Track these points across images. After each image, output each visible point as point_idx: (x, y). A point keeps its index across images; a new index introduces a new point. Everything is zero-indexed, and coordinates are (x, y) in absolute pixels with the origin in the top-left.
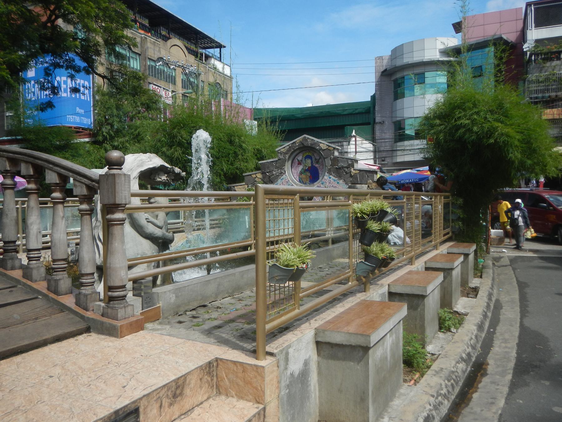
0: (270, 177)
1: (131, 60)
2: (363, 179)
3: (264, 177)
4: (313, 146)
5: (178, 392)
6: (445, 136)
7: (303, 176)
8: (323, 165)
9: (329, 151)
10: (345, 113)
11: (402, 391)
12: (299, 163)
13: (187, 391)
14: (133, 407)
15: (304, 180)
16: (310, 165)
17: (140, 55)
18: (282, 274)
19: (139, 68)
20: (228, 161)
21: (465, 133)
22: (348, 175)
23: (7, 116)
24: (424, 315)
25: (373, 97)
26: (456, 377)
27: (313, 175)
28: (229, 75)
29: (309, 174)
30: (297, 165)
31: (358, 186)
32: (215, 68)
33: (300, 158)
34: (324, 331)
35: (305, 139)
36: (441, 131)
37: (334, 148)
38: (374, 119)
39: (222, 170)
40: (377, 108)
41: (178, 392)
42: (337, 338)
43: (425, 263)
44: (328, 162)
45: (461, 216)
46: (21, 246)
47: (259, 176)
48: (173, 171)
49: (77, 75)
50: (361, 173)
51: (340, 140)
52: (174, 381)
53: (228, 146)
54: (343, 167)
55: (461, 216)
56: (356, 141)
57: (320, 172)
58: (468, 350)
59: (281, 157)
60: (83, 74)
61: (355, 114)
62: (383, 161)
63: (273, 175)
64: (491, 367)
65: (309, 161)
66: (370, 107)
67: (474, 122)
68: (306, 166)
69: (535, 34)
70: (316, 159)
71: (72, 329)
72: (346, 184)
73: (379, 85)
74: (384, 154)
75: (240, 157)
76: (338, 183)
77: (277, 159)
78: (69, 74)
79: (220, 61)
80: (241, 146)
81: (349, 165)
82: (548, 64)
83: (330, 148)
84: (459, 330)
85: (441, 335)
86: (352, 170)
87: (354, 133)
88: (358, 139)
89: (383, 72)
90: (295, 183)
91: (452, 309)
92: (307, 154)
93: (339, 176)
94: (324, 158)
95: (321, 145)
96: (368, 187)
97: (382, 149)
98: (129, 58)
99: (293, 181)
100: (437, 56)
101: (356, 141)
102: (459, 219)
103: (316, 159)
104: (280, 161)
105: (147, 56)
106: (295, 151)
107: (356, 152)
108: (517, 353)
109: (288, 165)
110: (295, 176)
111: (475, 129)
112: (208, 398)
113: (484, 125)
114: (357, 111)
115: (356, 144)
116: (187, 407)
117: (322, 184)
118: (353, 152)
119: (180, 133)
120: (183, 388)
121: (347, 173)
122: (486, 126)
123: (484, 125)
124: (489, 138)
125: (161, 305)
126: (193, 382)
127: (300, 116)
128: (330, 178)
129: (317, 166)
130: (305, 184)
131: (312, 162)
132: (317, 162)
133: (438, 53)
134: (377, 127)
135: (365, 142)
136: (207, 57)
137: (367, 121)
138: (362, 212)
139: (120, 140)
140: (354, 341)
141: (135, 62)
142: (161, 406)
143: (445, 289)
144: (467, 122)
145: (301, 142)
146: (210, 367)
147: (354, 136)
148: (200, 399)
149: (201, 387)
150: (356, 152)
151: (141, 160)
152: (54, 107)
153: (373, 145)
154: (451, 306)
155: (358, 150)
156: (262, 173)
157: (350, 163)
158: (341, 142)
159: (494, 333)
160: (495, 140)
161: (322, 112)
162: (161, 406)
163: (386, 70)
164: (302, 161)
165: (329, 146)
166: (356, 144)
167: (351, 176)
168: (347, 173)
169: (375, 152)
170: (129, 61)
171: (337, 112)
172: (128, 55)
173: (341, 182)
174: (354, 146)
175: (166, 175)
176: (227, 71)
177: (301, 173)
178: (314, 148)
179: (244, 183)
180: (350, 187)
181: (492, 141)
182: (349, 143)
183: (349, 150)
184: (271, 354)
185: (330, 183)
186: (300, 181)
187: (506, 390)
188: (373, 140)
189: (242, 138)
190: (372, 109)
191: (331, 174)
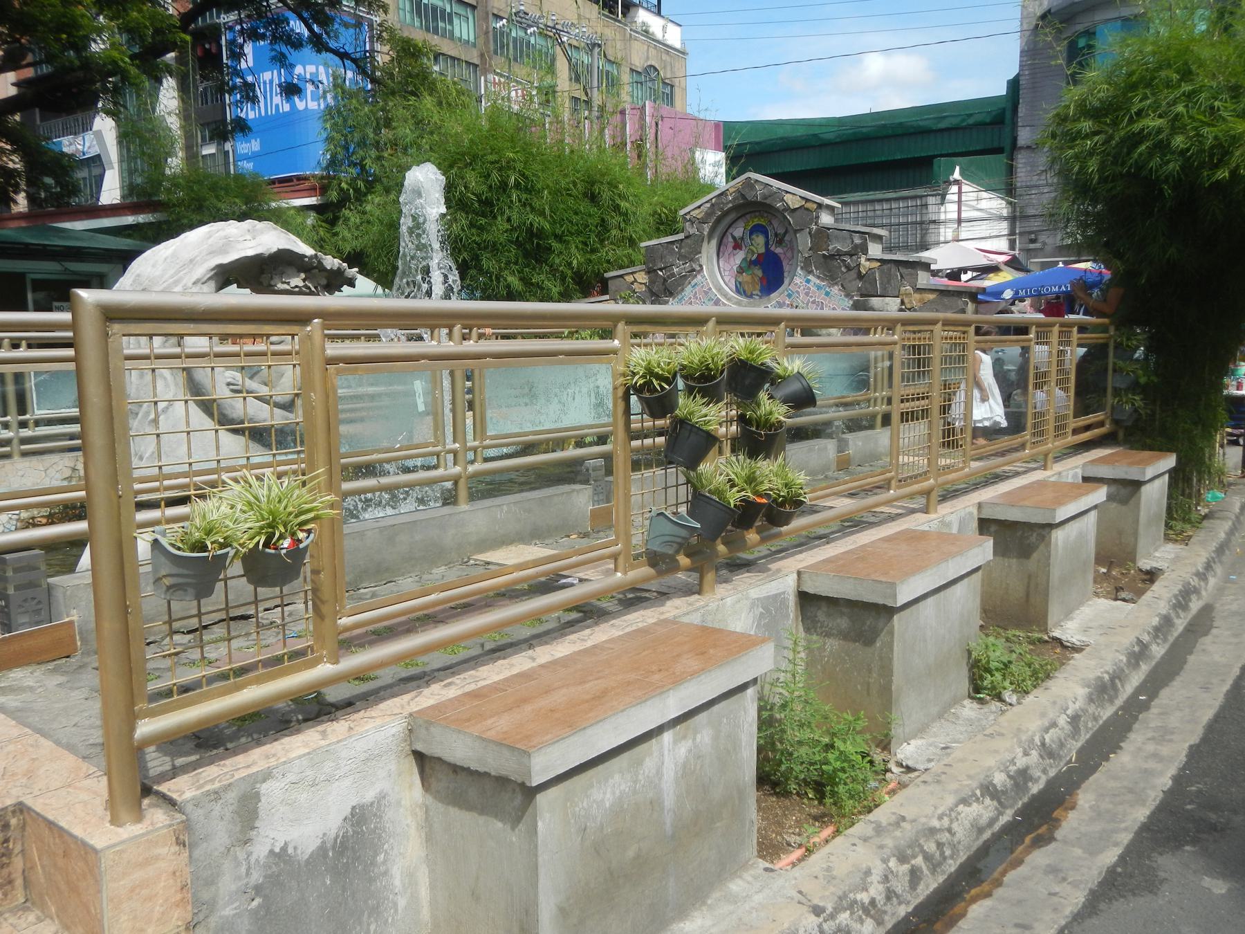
0: (665, 280)
1: (456, 21)
2: (889, 282)
3: (652, 282)
4: (768, 201)
6: (1102, 168)
7: (746, 277)
8: (792, 248)
9: (808, 213)
10: (942, 125)
11: (736, 886)
12: (737, 246)
15: (748, 288)
16: (762, 250)
17: (474, 7)
18: (175, 570)
19: (472, 38)
20: (585, 244)
21: (1150, 153)
22: (853, 274)
23: (203, 157)
24: (891, 660)
25: (1014, 85)
26: (940, 845)
27: (768, 273)
28: (678, 45)
29: (759, 273)
30: (730, 249)
31: (875, 301)
32: (647, 32)
33: (738, 232)
34: (429, 724)
35: (749, 184)
36: (1091, 153)
37: (820, 206)
38: (1015, 139)
39: (570, 264)
40: (1022, 111)
42: (457, 748)
43: (980, 505)
44: (804, 241)
45: (1143, 380)
46: (15, 442)
47: (642, 278)
48: (320, 263)
49: (293, 56)
50: (885, 267)
51: (920, 192)
53: (585, 206)
54: (839, 254)
55: (1143, 380)
56: (960, 193)
57: (786, 268)
58: (1021, 762)
59: (693, 230)
60: (308, 51)
61: (964, 128)
62: (1033, 241)
63: (673, 275)
64: (1072, 823)
65: (760, 240)
66: (1004, 110)
67: (1176, 124)
68: (753, 253)
70: (776, 235)
72: (847, 296)
73: (1031, 53)
74: (1035, 224)
75: (614, 232)
76: (827, 294)
78: (273, 53)
79: (659, 13)
80: (617, 208)
81: (856, 246)
83: (809, 205)
84: (1029, 699)
85: (969, 709)
86: (863, 260)
87: (957, 175)
88: (965, 188)
89: (1043, 17)
90: (725, 295)
91: (1046, 631)
92: (756, 221)
93: (831, 277)
94: (796, 231)
95: (787, 197)
96: (903, 303)
97: (1031, 211)
98: (450, 15)
99: (720, 289)
101: (960, 193)
102: (1135, 387)
103: (776, 235)
104: (688, 241)
105: (489, 8)
106: (725, 214)
107: (960, 221)
108: (1177, 779)
109: (708, 251)
110: (727, 279)
111: (1179, 141)
113: (1205, 130)
114: (971, 121)
115: (960, 202)
117: (789, 296)
118: (951, 221)
119: (463, 178)
121: (849, 269)
122: (1209, 133)
123: (1205, 130)
124: (1216, 166)
125: (75, 618)
127: (831, 136)
128: (808, 281)
129: (778, 250)
130: (751, 296)
131: (767, 244)
132: (780, 242)
134: (1021, 160)
135: (985, 195)
136: (628, 7)
137: (996, 145)
138: (650, 372)
139: (377, 200)
140: (496, 763)
141: (464, 25)
143: (1030, 577)
144: (1159, 122)
145: (738, 191)
147: (957, 182)
150: (960, 221)
151: (226, 237)
152: (250, 129)
153: (1010, 203)
154: (1046, 623)
155: (964, 215)
156: (650, 272)
157: (857, 241)
158: (921, 197)
159: (1145, 707)
160: (1234, 173)
161: (884, 126)
163: (1049, 11)
164: (742, 238)
165: (807, 200)
166: (960, 202)
167: (860, 277)
168: (849, 269)
169: (1012, 219)
170: (451, 22)
171: (921, 123)
172: (448, 10)
173: (836, 290)
174: (955, 207)
175: (303, 275)
176: (674, 37)
177: (741, 270)
178: (770, 207)
179: (607, 297)
180: (856, 306)
181: (1223, 174)
182: (943, 197)
183: (942, 217)
184: (172, 803)
185: (807, 294)
186: (738, 291)
187: (1076, 899)
188: (1009, 191)
189: (621, 186)
190: (1008, 115)
191: (810, 272)
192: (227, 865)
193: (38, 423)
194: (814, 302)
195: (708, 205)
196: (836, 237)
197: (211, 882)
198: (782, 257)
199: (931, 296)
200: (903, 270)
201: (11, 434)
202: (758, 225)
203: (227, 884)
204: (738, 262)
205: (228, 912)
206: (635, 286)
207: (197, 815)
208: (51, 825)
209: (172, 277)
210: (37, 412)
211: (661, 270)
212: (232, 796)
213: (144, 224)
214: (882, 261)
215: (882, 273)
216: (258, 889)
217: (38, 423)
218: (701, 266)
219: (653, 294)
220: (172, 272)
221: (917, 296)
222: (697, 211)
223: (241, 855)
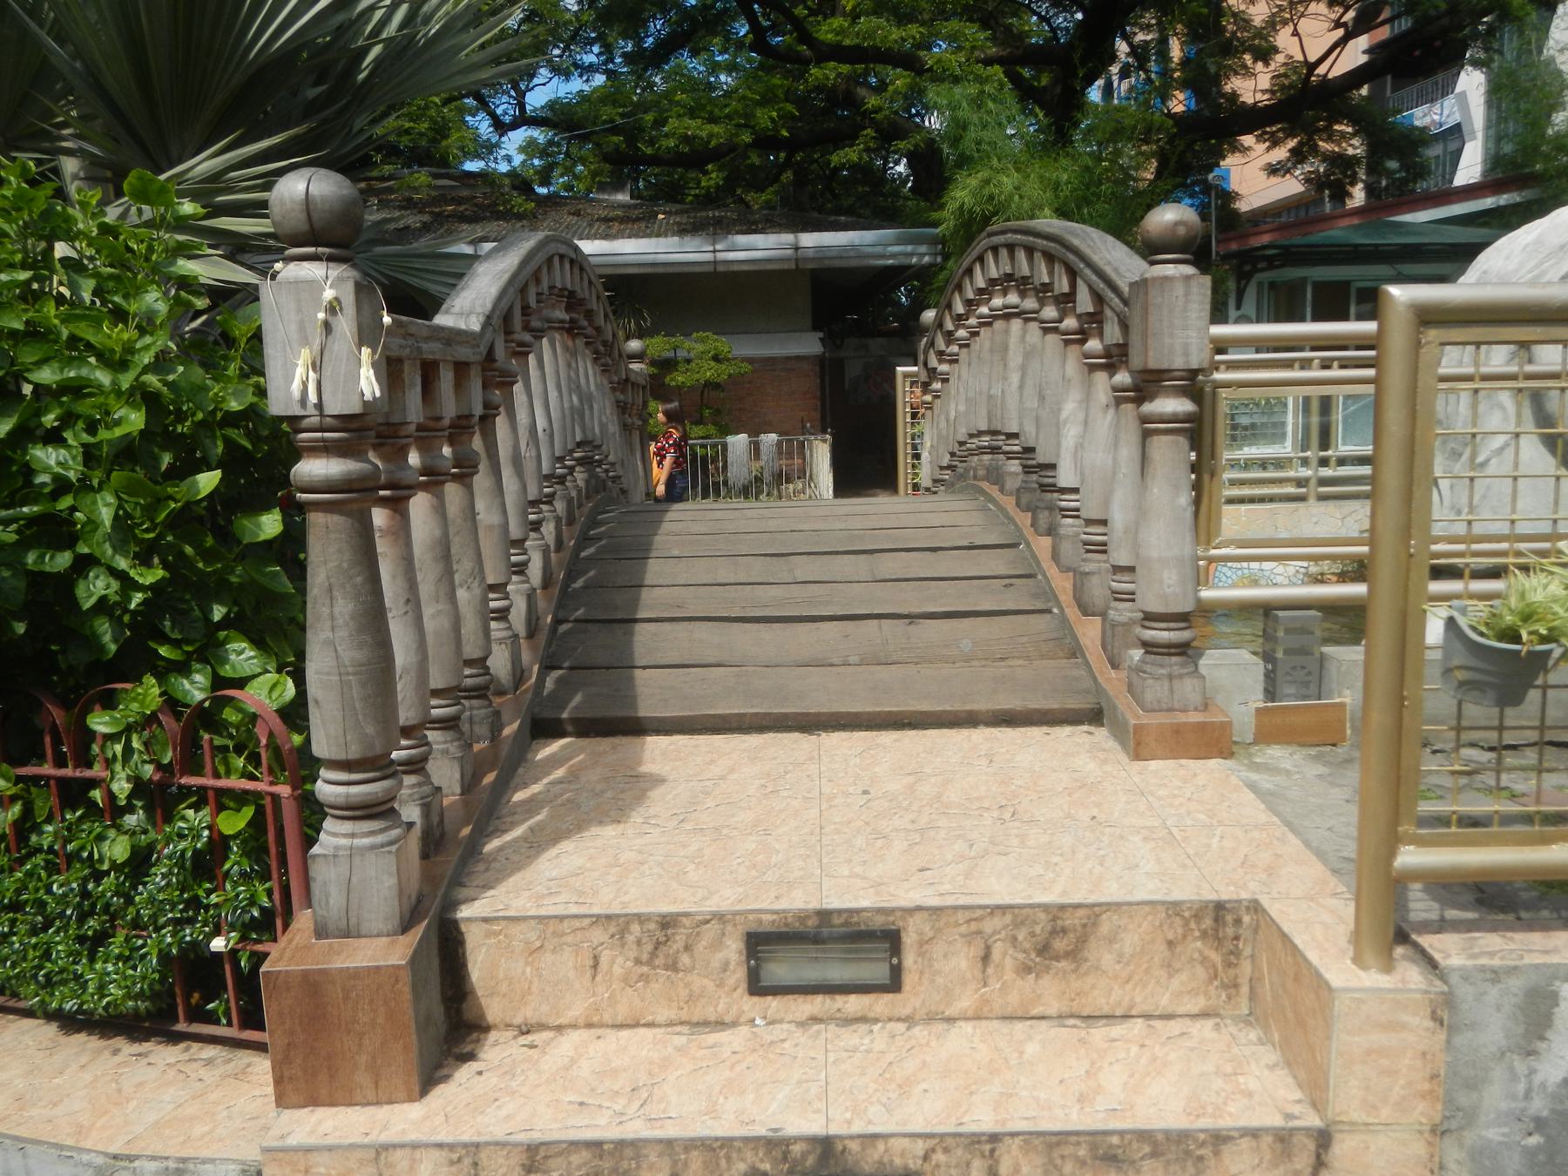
5: (1059, 945)
13: (1102, 956)
14: (878, 922)
18: (1473, 663)
41: (1059, 945)
46: (1313, 482)
52: (1045, 907)
71: (1053, 704)
112: (1204, 1015)
116: (1102, 1004)
120: (1082, 941)
125: (1348, 700)
126: (1130, 941)
142: (986, 958)
146: (1218, 920)
148: (1164, 1002)
149: (1171, 969)
162: (986, 958)
184: (1432, 964)
192: (1498, 1074)
193: (1342, 462)
197: (1473, 1085)
201: (1310, 473)
203: (1495, 1097)
205: (1493, 1134)
207: (1465, 992)
208: (1285, 937)
209: (1530, 272)
210: (1341, 448)
212: (1516, 984)
213: (1505, 207)
216: (1540, 1124)
217: (1342, 462)
220: (1532, 264)
223: (1521, 1067)
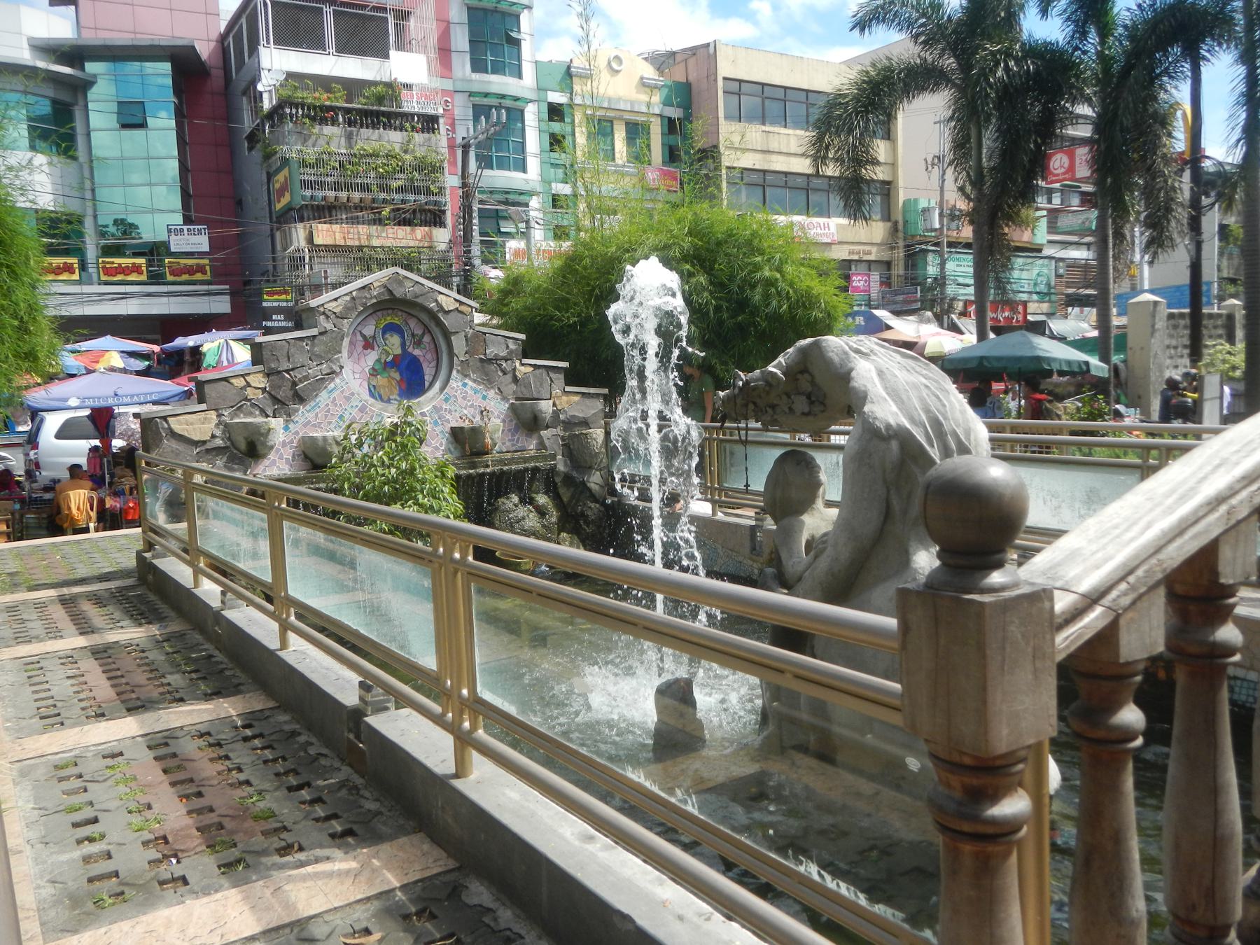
2: (541, 385)
4: (419, 300)
7: (381, 380)
12: (368, 345)
16: (398, 351)
22: (509, 377)
27: (410, 378)
29: (397, 376)
30: (360, 349)
44: (459, 344)
57: (428, 372)
59: (329, 326)
65: (394, 341)
68: (388, 354)
69: (277, 64)
70: (413, 335)
72: (504, 399)
76: (484, 398)
77: (314, 332)
81: (511, 352)
82: (316, 129)
83: (462, 308)
92: (389, 320)
93: (488, 381)
95: (441, 298)
96: (554, 405)
100: (25, 56)
103: (413, 335)
104: (324, 338)
117: (446, 400)
128: (465, 385)
129: (417, 352)
130: (389, 401)
131: (403, 345)
132: (418, 343)
133: (26, 46)
164: (374, 337)
165: (462, 303)
167: (515, 380)
168: (505, 373)
173: (492, 393)
177: (374, 372)
179: (204, 407)
194: (471, 406)
195: (348, 298)
196: (493, 342)
198: (421, 359)
199: (576, 398)
200: (552, 375)
202: (392, 324)
204: (371, 363)
206: (250, 392)
211: (287, 371)
214: (536, 367)
215: (535, 376)
218: (342, 367)
219: (275, 400)
221: (565, 398)
222: (334, 304)
